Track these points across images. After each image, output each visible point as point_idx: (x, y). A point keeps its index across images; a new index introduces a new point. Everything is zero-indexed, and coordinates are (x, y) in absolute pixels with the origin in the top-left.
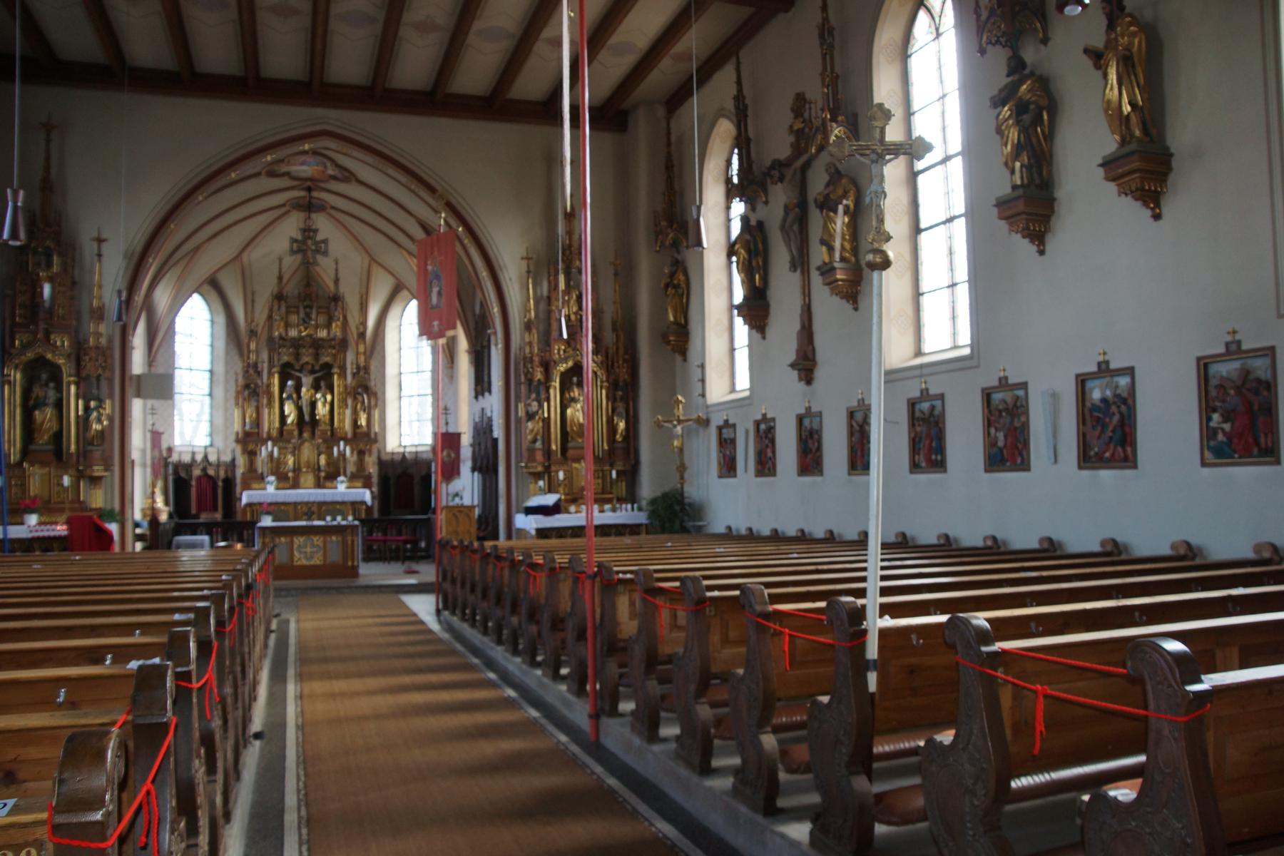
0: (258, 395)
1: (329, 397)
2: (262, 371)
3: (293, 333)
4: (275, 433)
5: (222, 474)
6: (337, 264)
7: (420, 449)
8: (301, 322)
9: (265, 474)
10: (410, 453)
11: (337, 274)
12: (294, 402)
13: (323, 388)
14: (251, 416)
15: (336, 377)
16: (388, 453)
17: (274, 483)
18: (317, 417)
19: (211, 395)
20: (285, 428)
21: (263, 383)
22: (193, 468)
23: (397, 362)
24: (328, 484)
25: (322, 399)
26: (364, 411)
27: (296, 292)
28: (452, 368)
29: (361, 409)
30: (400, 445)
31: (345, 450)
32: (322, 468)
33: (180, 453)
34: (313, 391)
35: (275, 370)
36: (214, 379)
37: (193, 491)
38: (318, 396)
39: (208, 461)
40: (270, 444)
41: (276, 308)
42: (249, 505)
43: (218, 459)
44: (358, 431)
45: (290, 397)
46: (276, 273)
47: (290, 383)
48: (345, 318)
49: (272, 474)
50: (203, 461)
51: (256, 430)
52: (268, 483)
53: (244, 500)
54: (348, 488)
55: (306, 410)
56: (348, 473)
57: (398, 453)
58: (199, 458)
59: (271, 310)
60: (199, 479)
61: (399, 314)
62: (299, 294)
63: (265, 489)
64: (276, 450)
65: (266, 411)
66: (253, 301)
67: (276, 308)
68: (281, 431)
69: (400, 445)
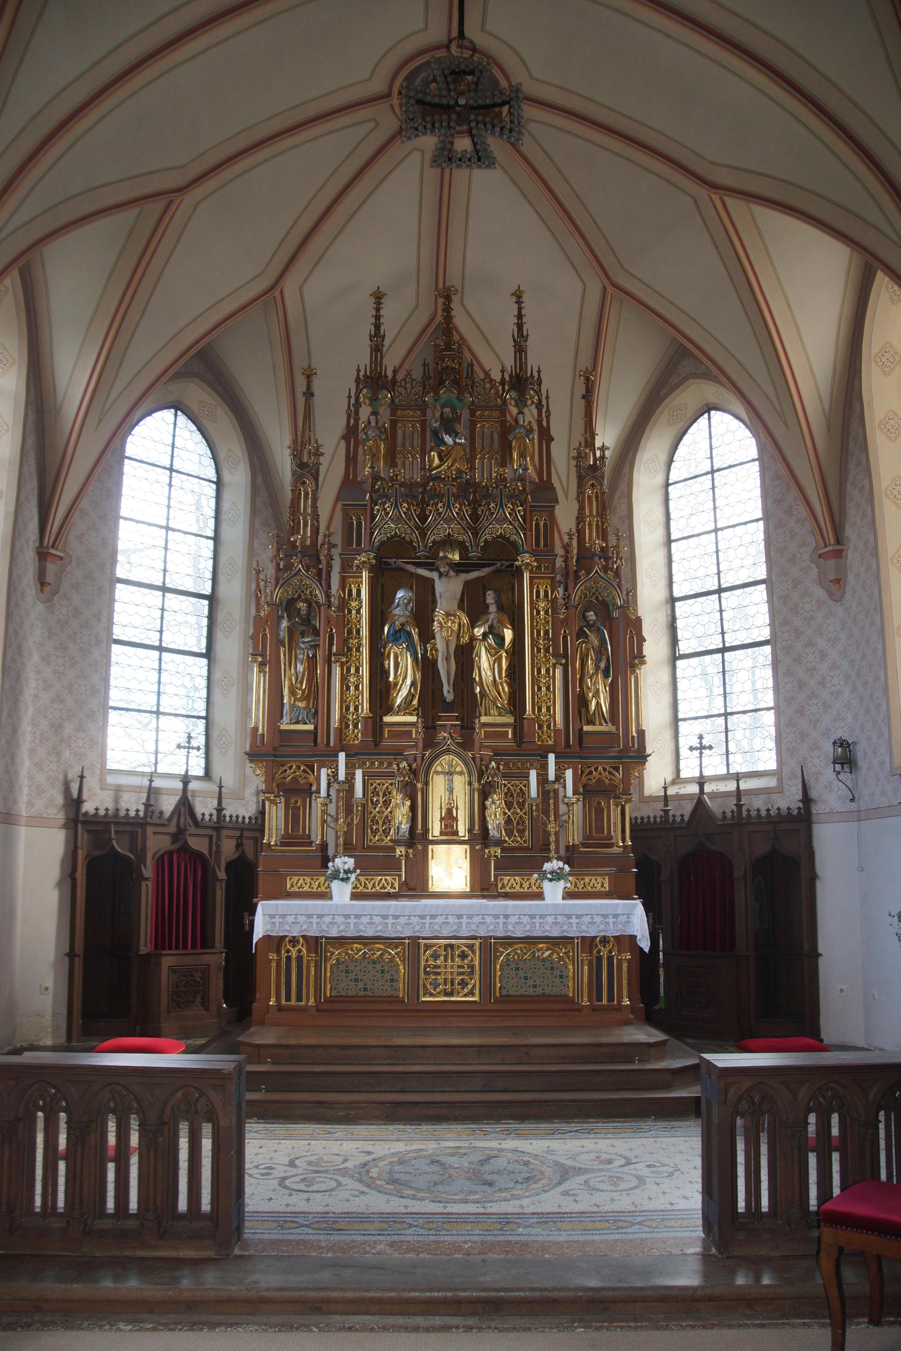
0: (316, 633)
1: (508, 634)
2: (330, 567)
3: (409, 471)
4: (356, 736)
5: (228, 849)
6: (519, 303)
7: (744, 785)
8: (429, 444)
9: (331, 852)
10: (714, 795)
11: (520, 326)
12: (411, 648)
13: (493, 608)
14: (292, 692)
15: (526, 576)
16: (652, 799)
17: (353, 877)
18: (478, 690)
19: (209, 654)
20: (387, 719)
21: (328, 596)
22: (150, 830)
23: (664, 572)
24: (512, 882)
25: (491, 640)
26: (606, 675)
27: (418, 375)
28: (839, 554)
29: (597, 668)
30: (677, 779)
31: (559, 778)
32: (493, 833)
33: (118, 790)
34: (465, 620)
35: (363, 558)
36: (221, 616)
37: (147, 893)
38: (479, 632)
39: (192, 813)
40: (342, 756)
41: (365, 412)
42: (275, 942)
43: (220, 810)
44: (586, 728)
45: (399, 635)
46: (368, 327)
47: (400, 594)
48: (546, 436)
49: (348, 849)
50: (177, 811)
51: (310, 727)
52: (335, 876)
53: (259, 932)
54: (569, 895)
55: (445, 669)
56: (562, 852)
57: (679, 797)
58: (168, 805)
59: (353, 412)
60: (164, 861)
61: (663, 457)
62: (426, 377)
63: (326, 895)
64: (359, 774)
65: (337, 671)
66: (309, 394)
67: (365, 412)
68: (375, 726)
69: (677, 779)
